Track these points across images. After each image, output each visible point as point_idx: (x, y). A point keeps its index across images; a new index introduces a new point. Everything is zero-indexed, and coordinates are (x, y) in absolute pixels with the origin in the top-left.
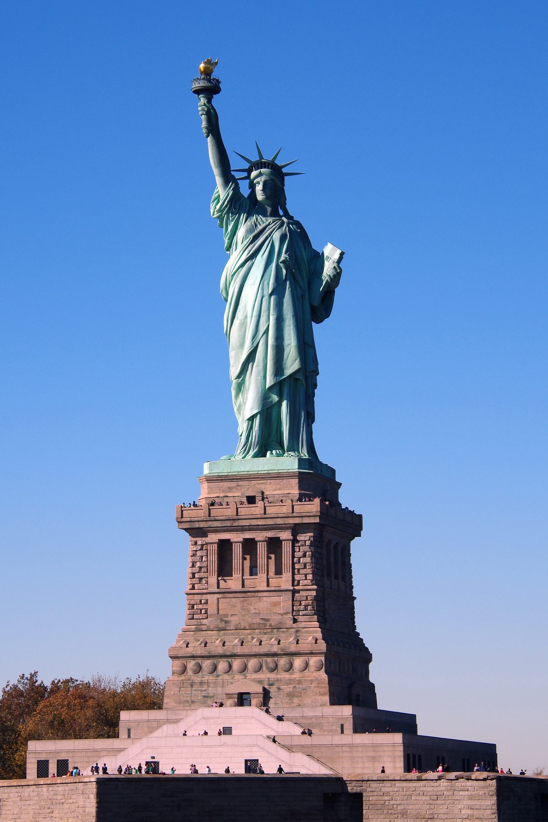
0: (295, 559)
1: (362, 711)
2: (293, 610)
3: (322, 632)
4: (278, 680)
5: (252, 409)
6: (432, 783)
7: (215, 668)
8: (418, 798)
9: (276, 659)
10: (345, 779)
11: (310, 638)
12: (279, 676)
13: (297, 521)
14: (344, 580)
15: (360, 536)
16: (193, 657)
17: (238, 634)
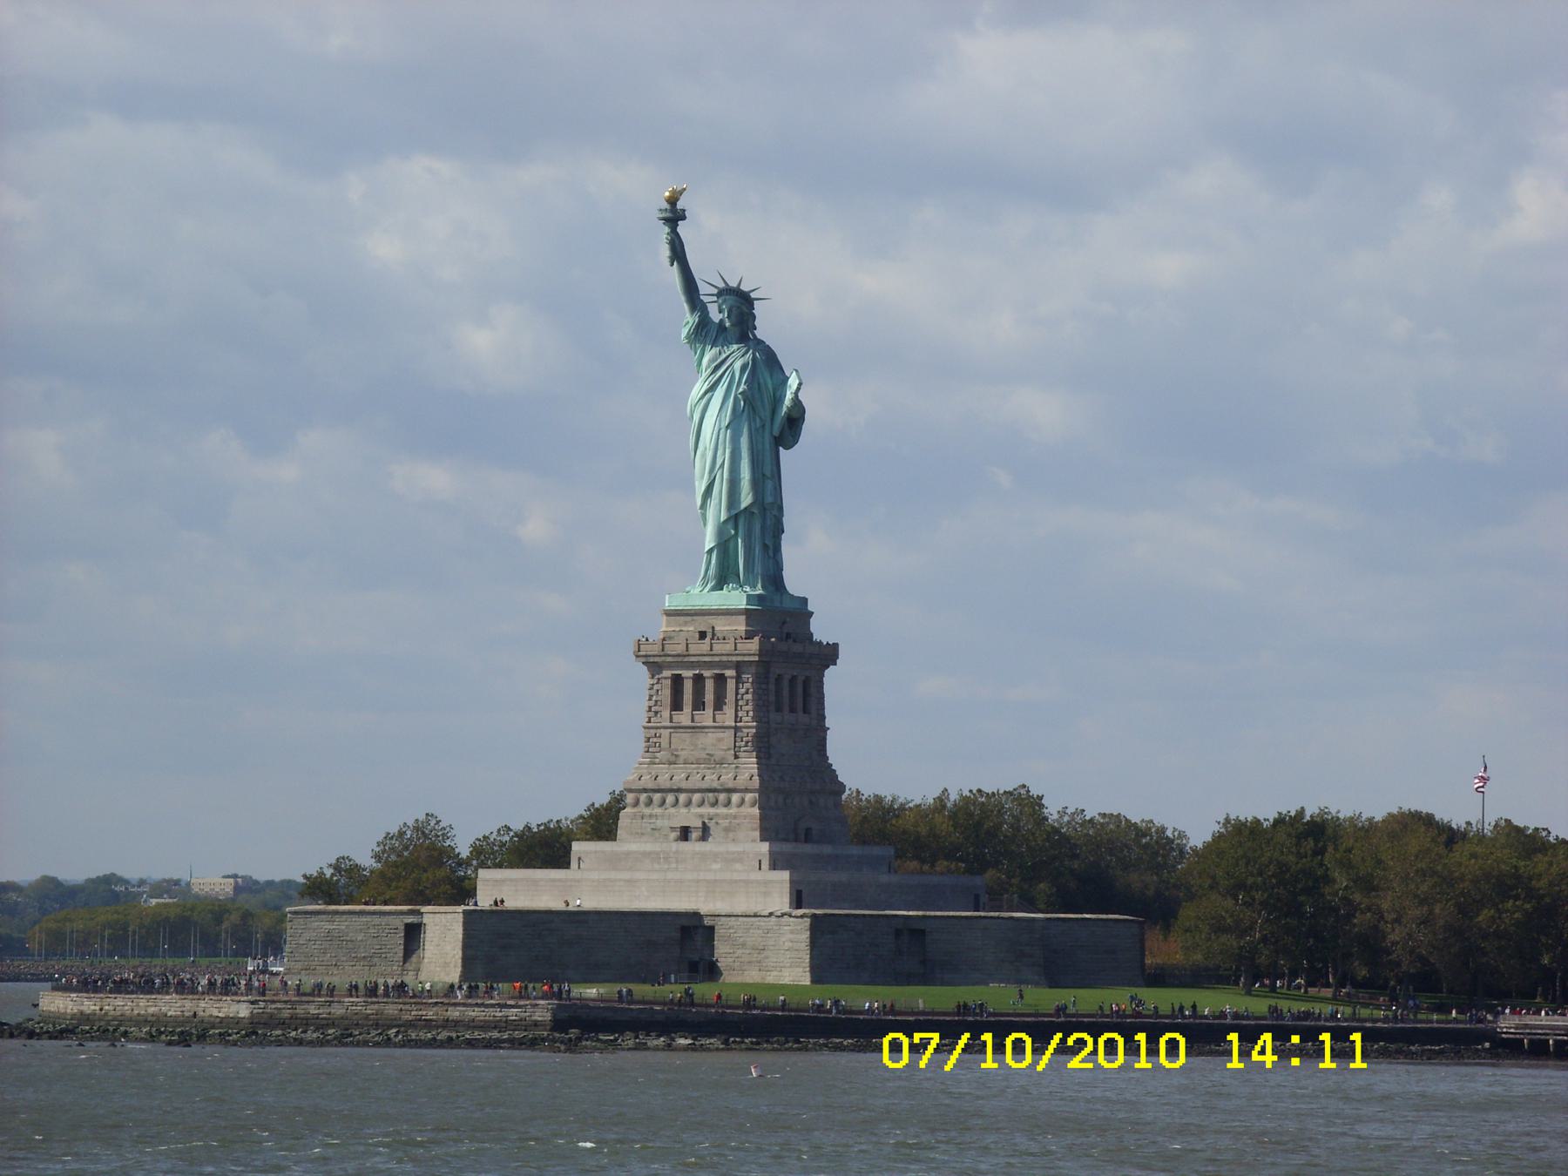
0: (739, 697)
1: (787, 847)
2: (735, 746)
3: (758, 768)
4: (717, 815)
5: (709, 542)
6: (765, 919)
7: (663, 802)
8: (754, 931)
9: (716, 794)
10: (702, 914)
11: (747, 775)
12: (718, 811)
13: (740, 659)
14: (805, 711)
15: (835, 664)
16: (645, 790)
17: (686, 768)
